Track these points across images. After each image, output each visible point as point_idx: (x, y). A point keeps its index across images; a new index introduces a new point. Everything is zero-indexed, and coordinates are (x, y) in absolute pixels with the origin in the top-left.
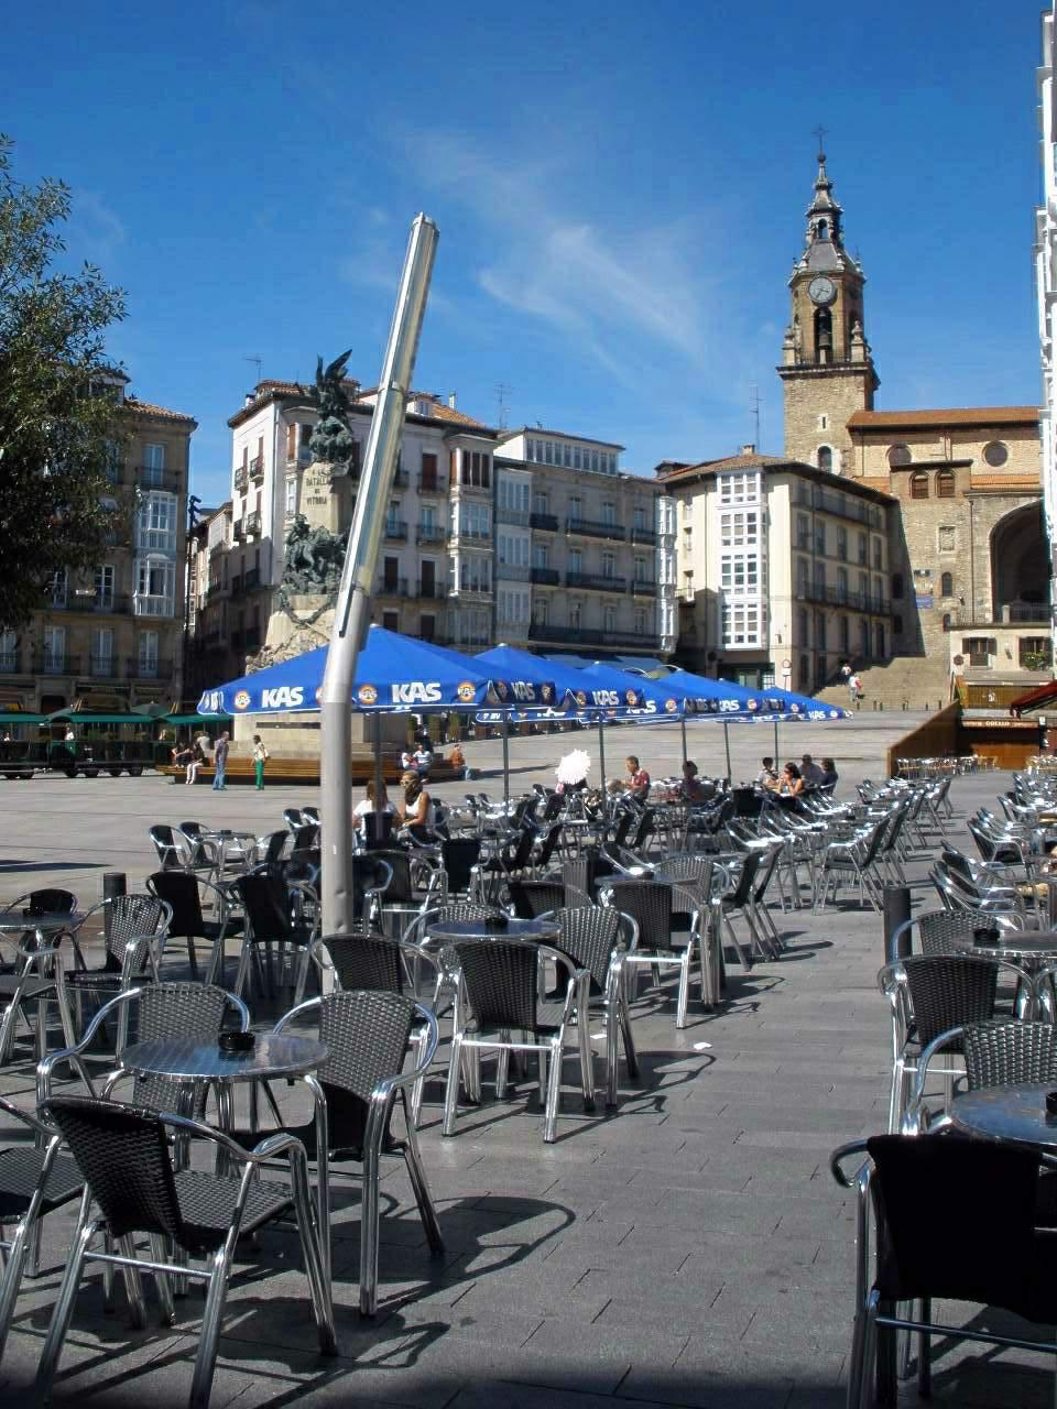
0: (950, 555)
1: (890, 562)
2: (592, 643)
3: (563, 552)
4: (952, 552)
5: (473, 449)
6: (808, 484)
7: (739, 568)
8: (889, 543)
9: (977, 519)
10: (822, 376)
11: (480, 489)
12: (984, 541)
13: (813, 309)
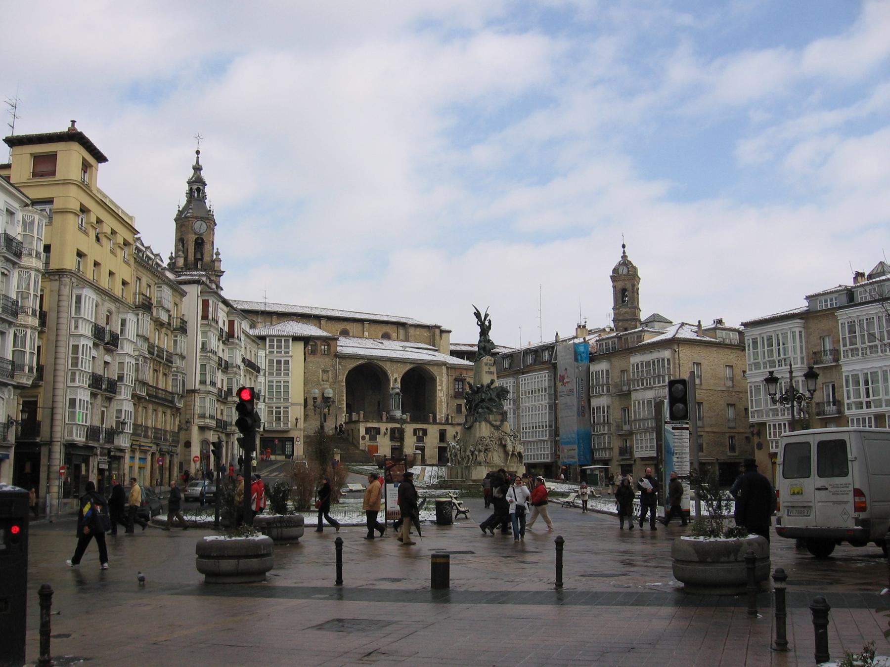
7: (279, 387)
12: (343, 378)
13: (194, 237)
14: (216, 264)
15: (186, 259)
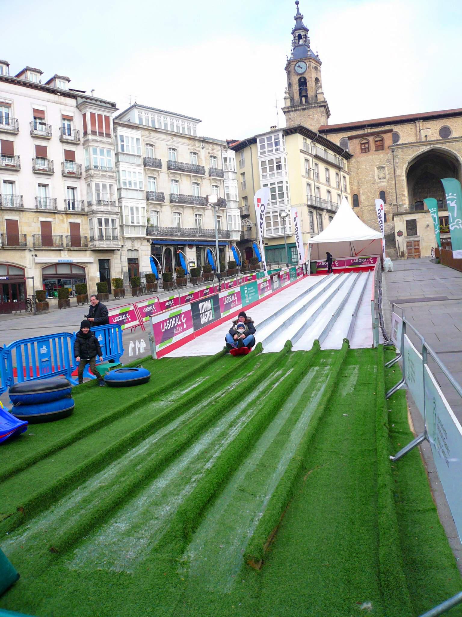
0: (383, 182)
1: (351, 189)
2: (190, 236)
3: (165, 184)
4: (384, 180)
5: (97, 112)
6: (309, 141)
8: (350, 179)
9: (397, 161)
10: (304, 109)
11: (105, 139)
12: (402, 172)
14: (319, 96)
15: (292, 100)
